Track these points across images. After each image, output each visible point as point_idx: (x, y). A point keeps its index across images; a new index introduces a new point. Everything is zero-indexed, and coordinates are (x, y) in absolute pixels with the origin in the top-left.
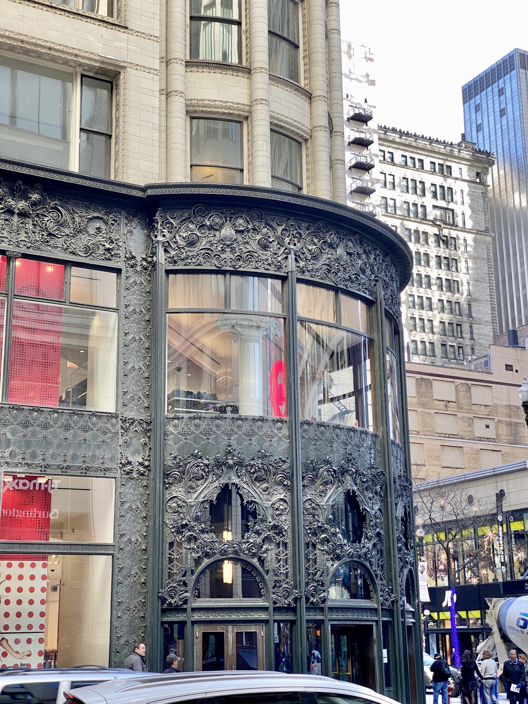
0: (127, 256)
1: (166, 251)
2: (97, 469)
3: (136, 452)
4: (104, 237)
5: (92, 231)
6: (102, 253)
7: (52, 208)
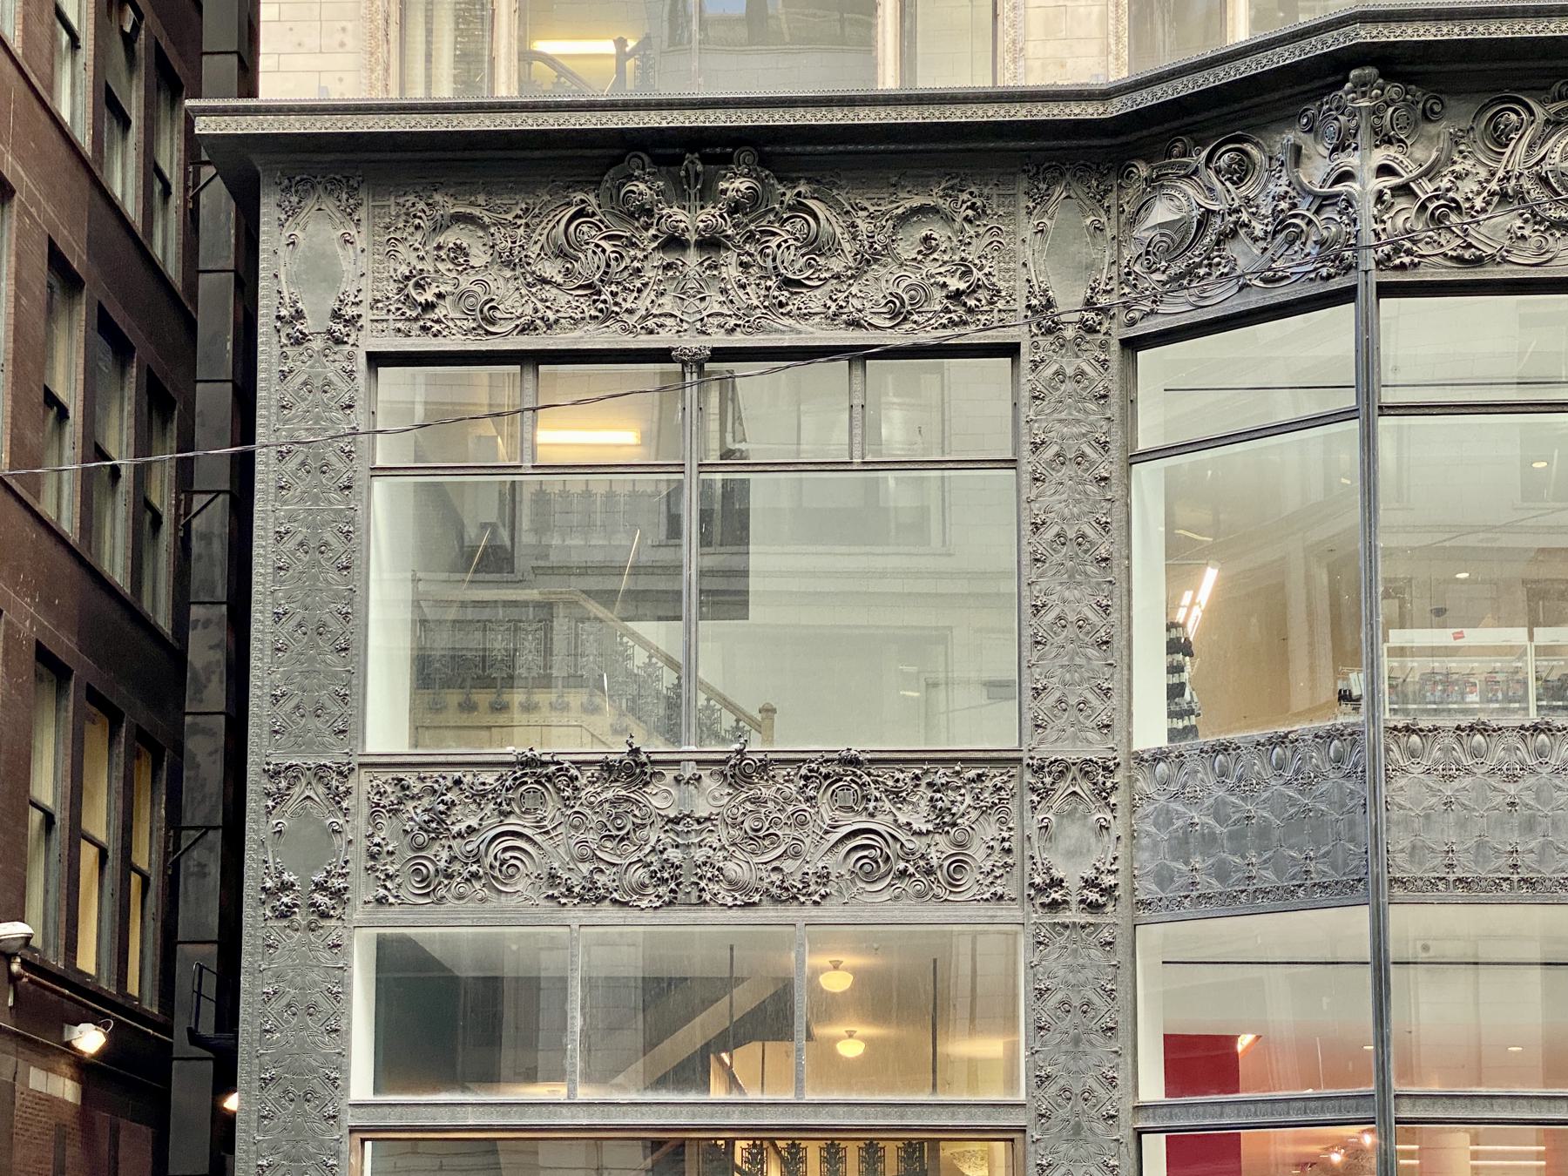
0: (1034, 302)
4: (945, 263)
6: (938, 308)
7: (790, 208)
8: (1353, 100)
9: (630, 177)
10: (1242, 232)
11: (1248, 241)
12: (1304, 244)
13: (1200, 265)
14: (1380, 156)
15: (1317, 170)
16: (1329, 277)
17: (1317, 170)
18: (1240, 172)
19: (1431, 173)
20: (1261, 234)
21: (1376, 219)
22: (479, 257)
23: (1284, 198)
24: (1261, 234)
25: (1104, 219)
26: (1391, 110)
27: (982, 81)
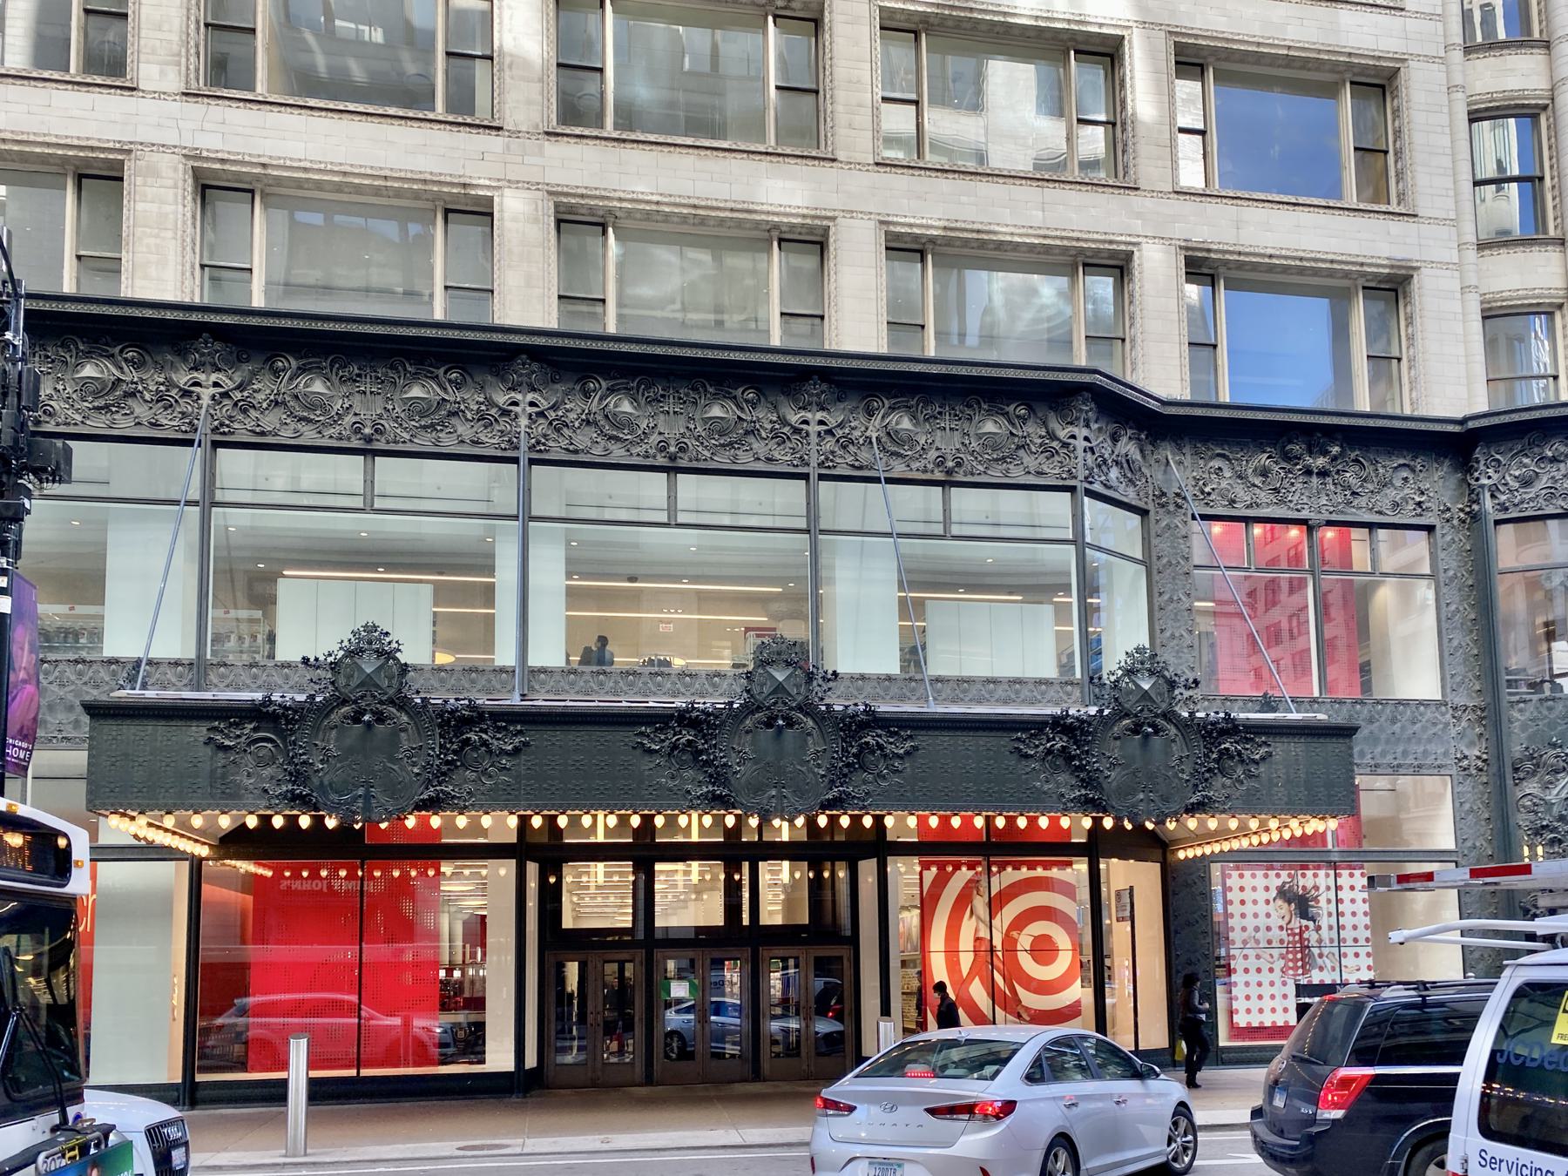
1: (1493, 496)
2: (1431, 766)
3: (1471, 744)
5: (1398, 483)
9: (1290, 442)
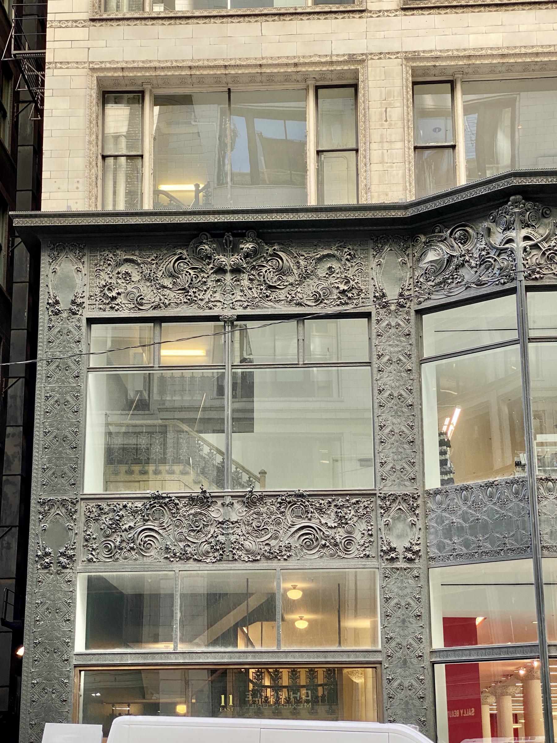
0: (377, 294)
4: (338, 278)
6: (335, 297)
7: (270, 255)
8: (512, 209)
9: (202, 243)
10: (466, 264)
11: (469, 268)
12: (493, 269)
13: (448, 278)
14: (524, 232)
15: (497, 238)
16: (505, 283)
17: (497, 238)
18: (465, 239)
19: (546, 239)
20: (474, 265)
21: (523, 260)
22: (136, 277)
23: (484, 250)
24: (474, 265)
25: (406, 259)
26: (528, 213)
27: (353, 202)
